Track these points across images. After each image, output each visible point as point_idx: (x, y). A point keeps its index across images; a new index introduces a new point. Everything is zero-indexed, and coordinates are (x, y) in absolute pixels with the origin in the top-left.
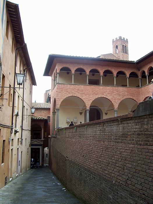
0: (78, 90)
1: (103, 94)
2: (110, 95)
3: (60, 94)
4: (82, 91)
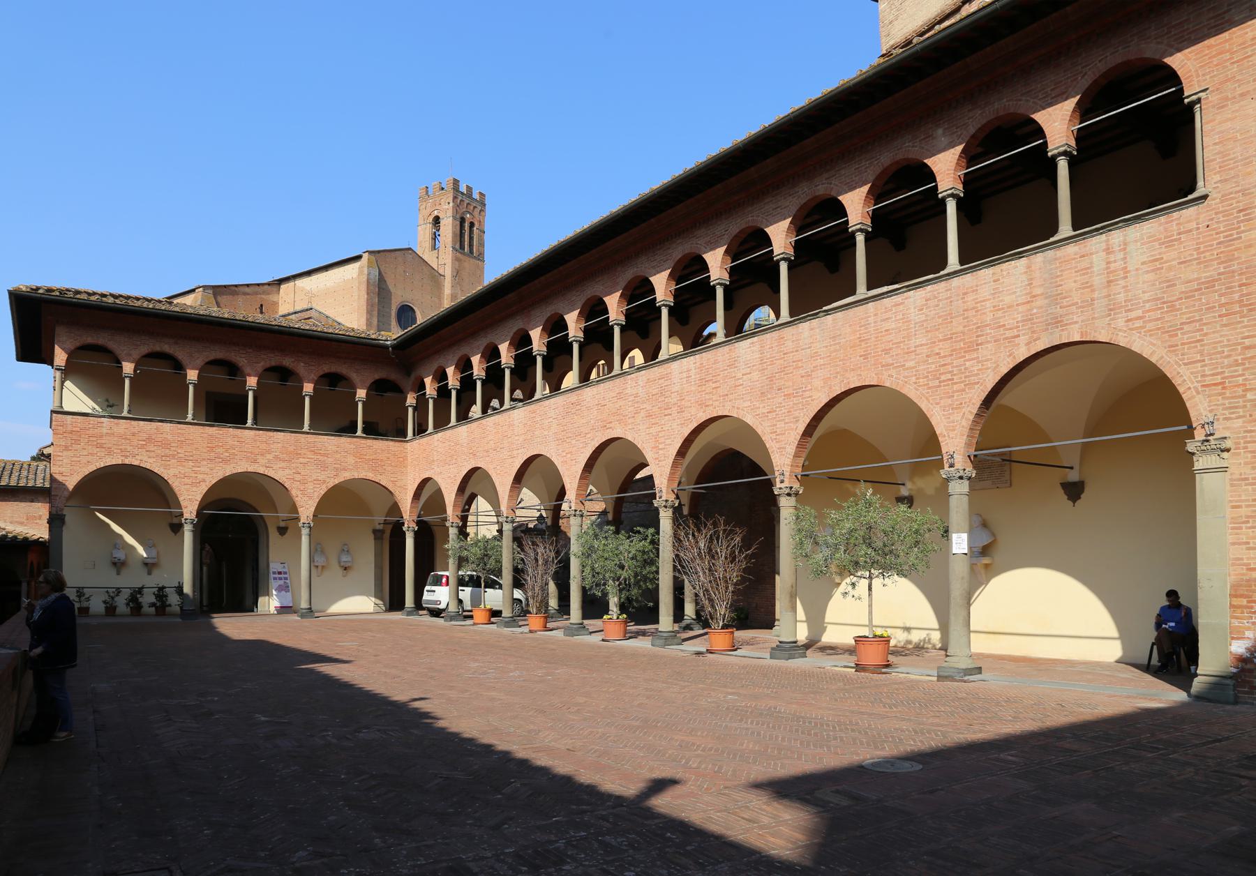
0: (149, 439)
1: (255, 461)
2: (283, 465)
3: (65, 453)
4: (166, 445)
